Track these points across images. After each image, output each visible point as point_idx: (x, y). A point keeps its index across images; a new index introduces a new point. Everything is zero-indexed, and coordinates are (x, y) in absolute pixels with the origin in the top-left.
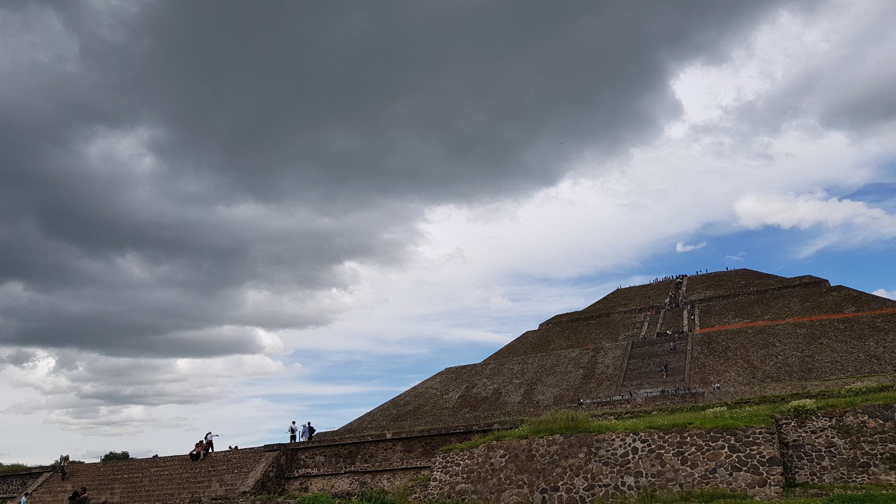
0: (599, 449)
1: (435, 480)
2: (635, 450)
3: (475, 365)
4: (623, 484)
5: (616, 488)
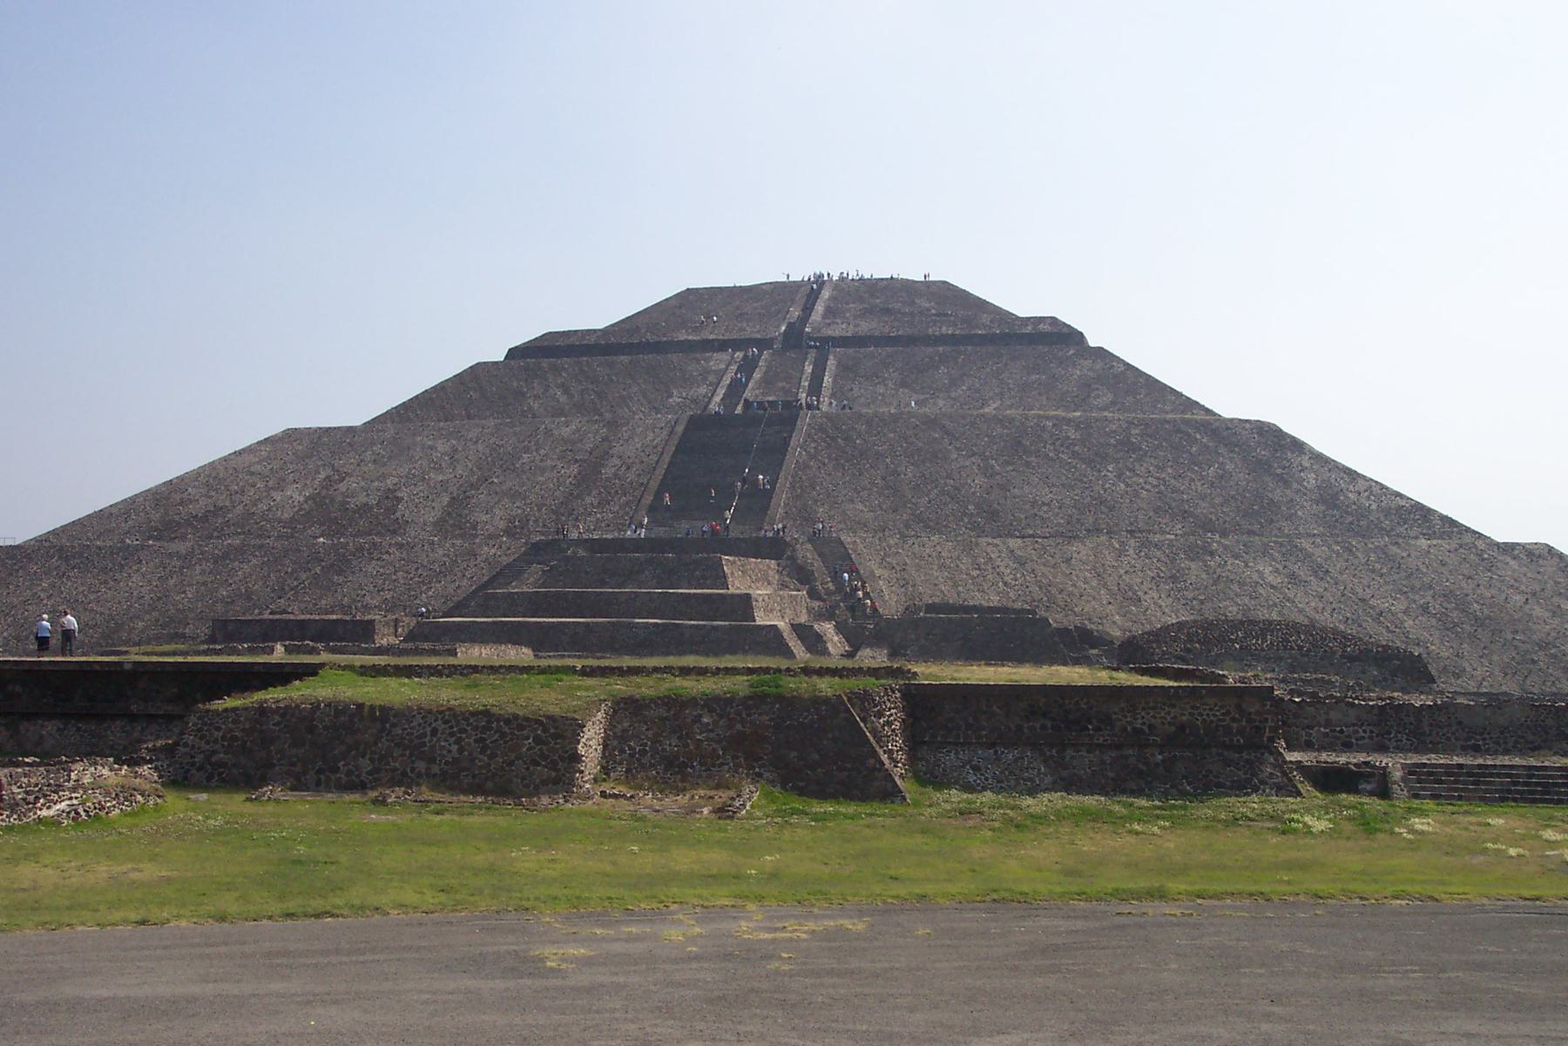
0: (394, 725)
1: (186, 745)
2: (434, 732)
3: (351, 430)
4: (413, 770)
5: (404, 774)
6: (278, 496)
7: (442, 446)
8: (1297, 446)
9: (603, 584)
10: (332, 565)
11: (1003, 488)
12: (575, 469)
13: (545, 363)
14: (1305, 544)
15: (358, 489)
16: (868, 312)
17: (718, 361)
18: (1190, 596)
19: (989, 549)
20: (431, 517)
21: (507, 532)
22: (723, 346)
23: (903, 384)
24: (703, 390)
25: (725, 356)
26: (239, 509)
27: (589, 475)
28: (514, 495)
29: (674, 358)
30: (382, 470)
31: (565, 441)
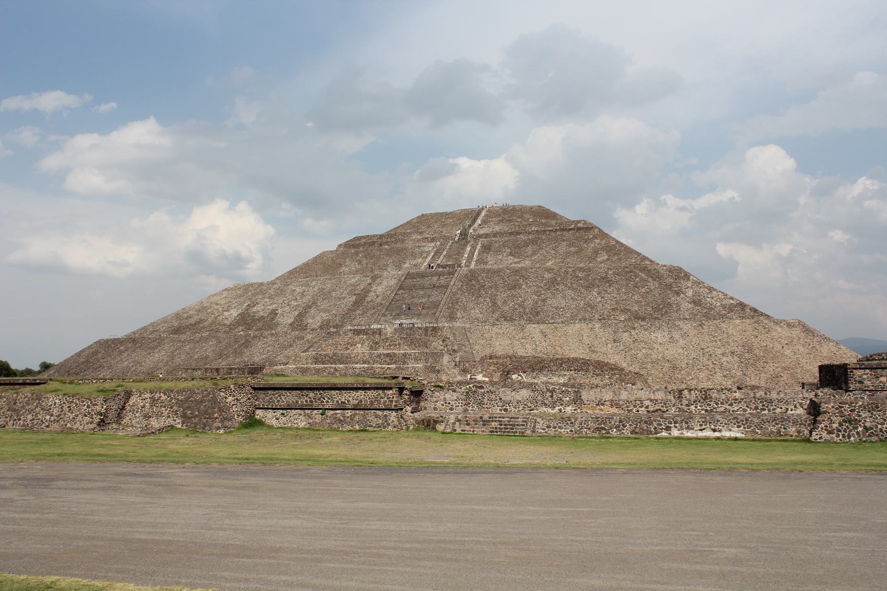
6: (226, 313)
7: (298, 290)
12: (354, 297)
15: (261, 309)
20: (290, 321)
23: (511, 254)
24: (420, 260)
28: (325, 311)
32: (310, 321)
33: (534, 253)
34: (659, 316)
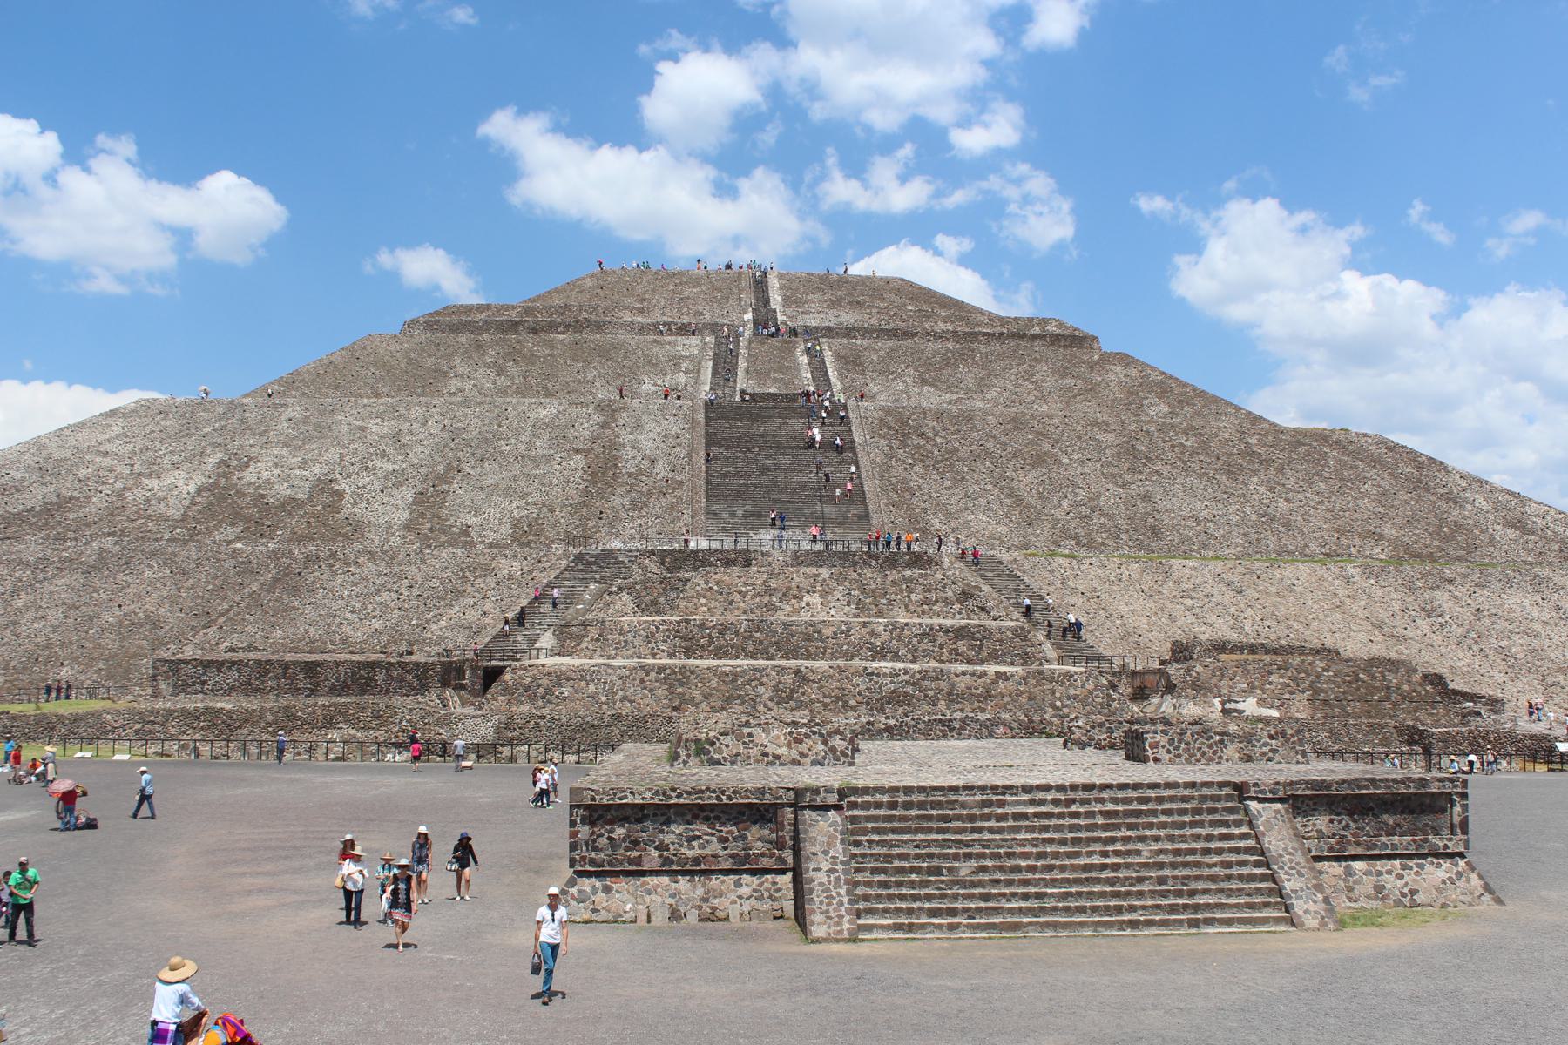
6: (153, 483)
8: (1442, 466)
9: (772, 608)
10: (276, 580)
11: (1147, 497)
13: (463, 339)
14: (1545, 572)
16: (835, 303)
17: (690, 346)
18: (1459, 631)
19: (1187, 571)
20: (401, 516)
21: (515, 538)
22: (684, 330)
23: (924, 382)
25: (695, 341)
26: (98, 503)
27: (603, 467)
28: (506, 493)
29: (632, 340)
30: (300, 454)
31: (550, 425)
32: (470, 519)
33: (982, 386)
34: (1462, 553)
